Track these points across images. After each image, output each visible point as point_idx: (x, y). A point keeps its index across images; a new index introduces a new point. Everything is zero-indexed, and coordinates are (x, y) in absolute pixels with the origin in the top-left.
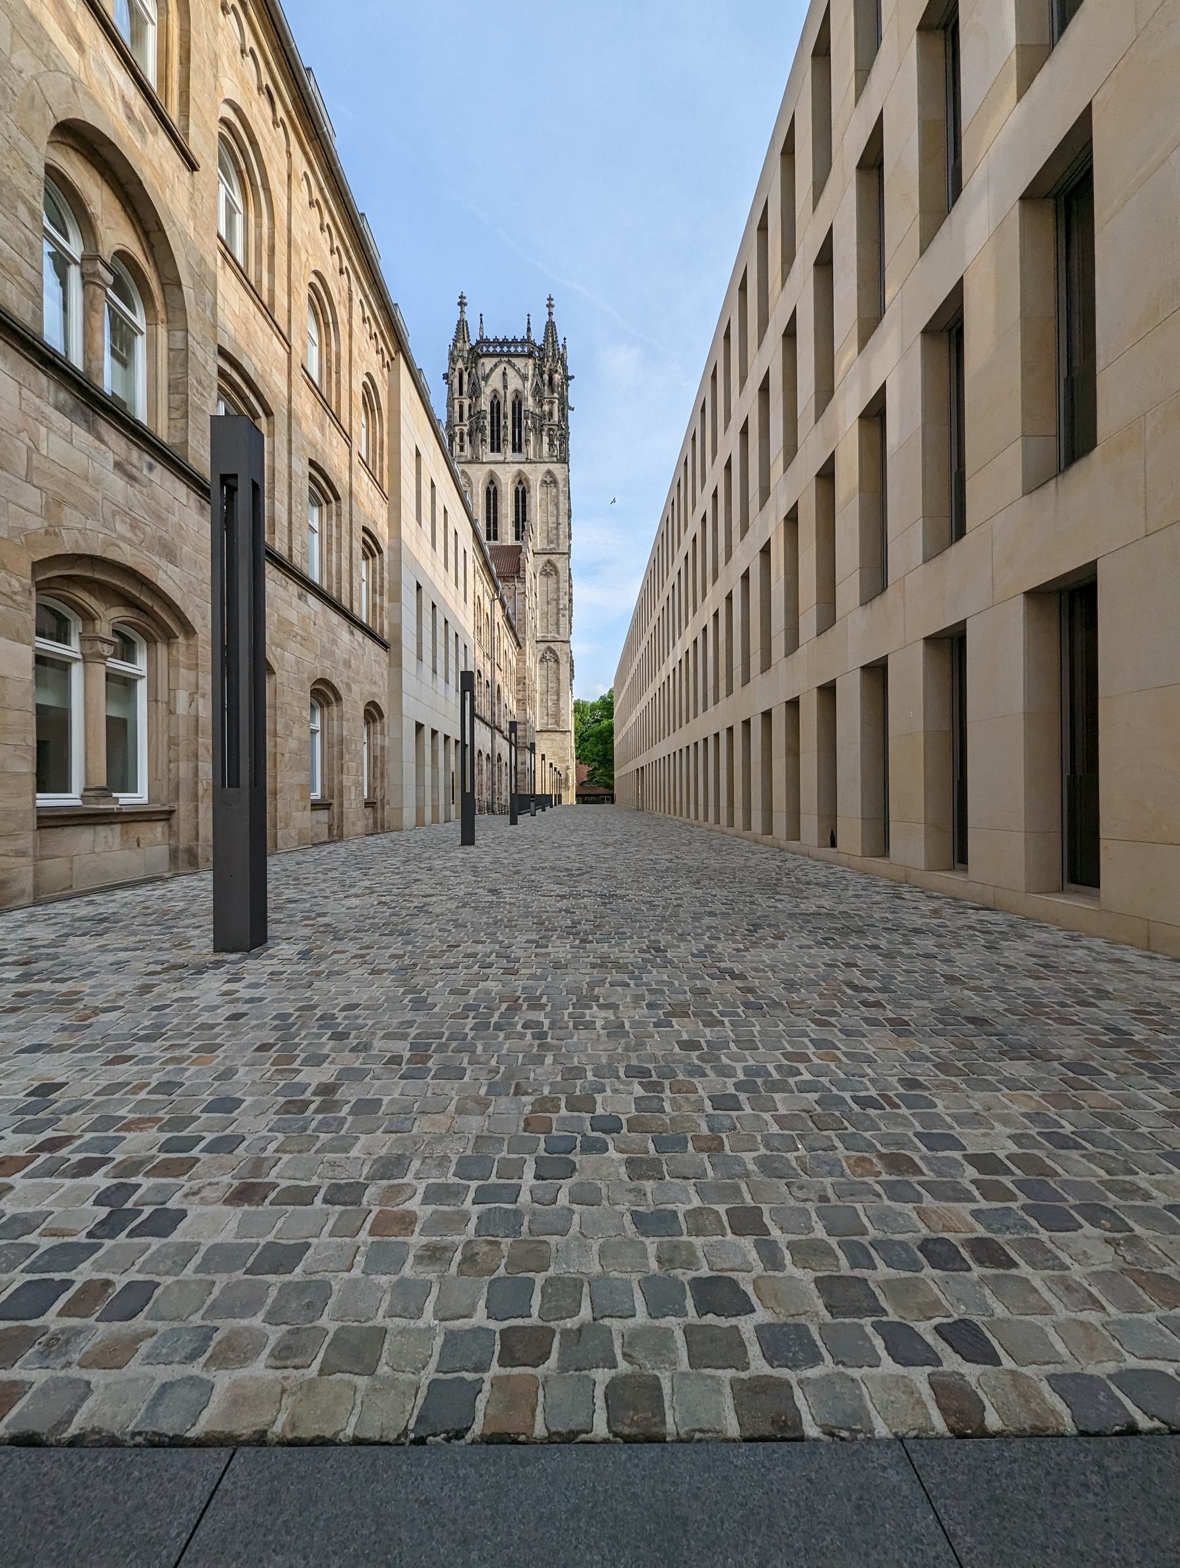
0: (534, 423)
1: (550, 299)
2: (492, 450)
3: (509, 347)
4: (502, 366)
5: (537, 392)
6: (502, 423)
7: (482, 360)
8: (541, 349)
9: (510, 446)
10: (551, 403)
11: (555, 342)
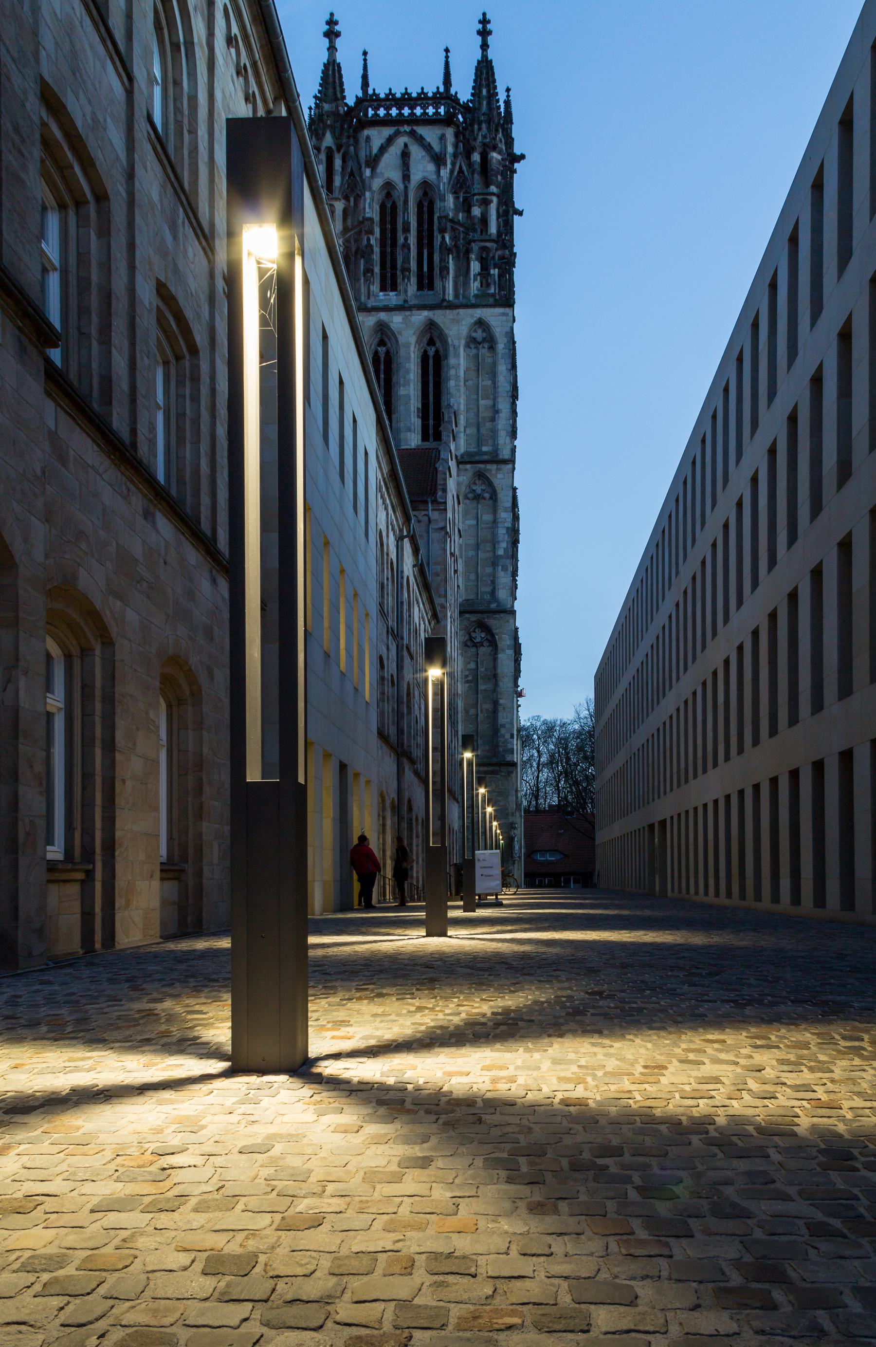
0: (454, 238)
1: (484, 21)
2: (383, 288)
3: (412, 108)
4: (401, 141)
5: (459, 184)
6: (401, 240)
7: (366, 132)
8: (465, 108)
9: (414, 280)
10: (486, 203)
11: (492, 95)
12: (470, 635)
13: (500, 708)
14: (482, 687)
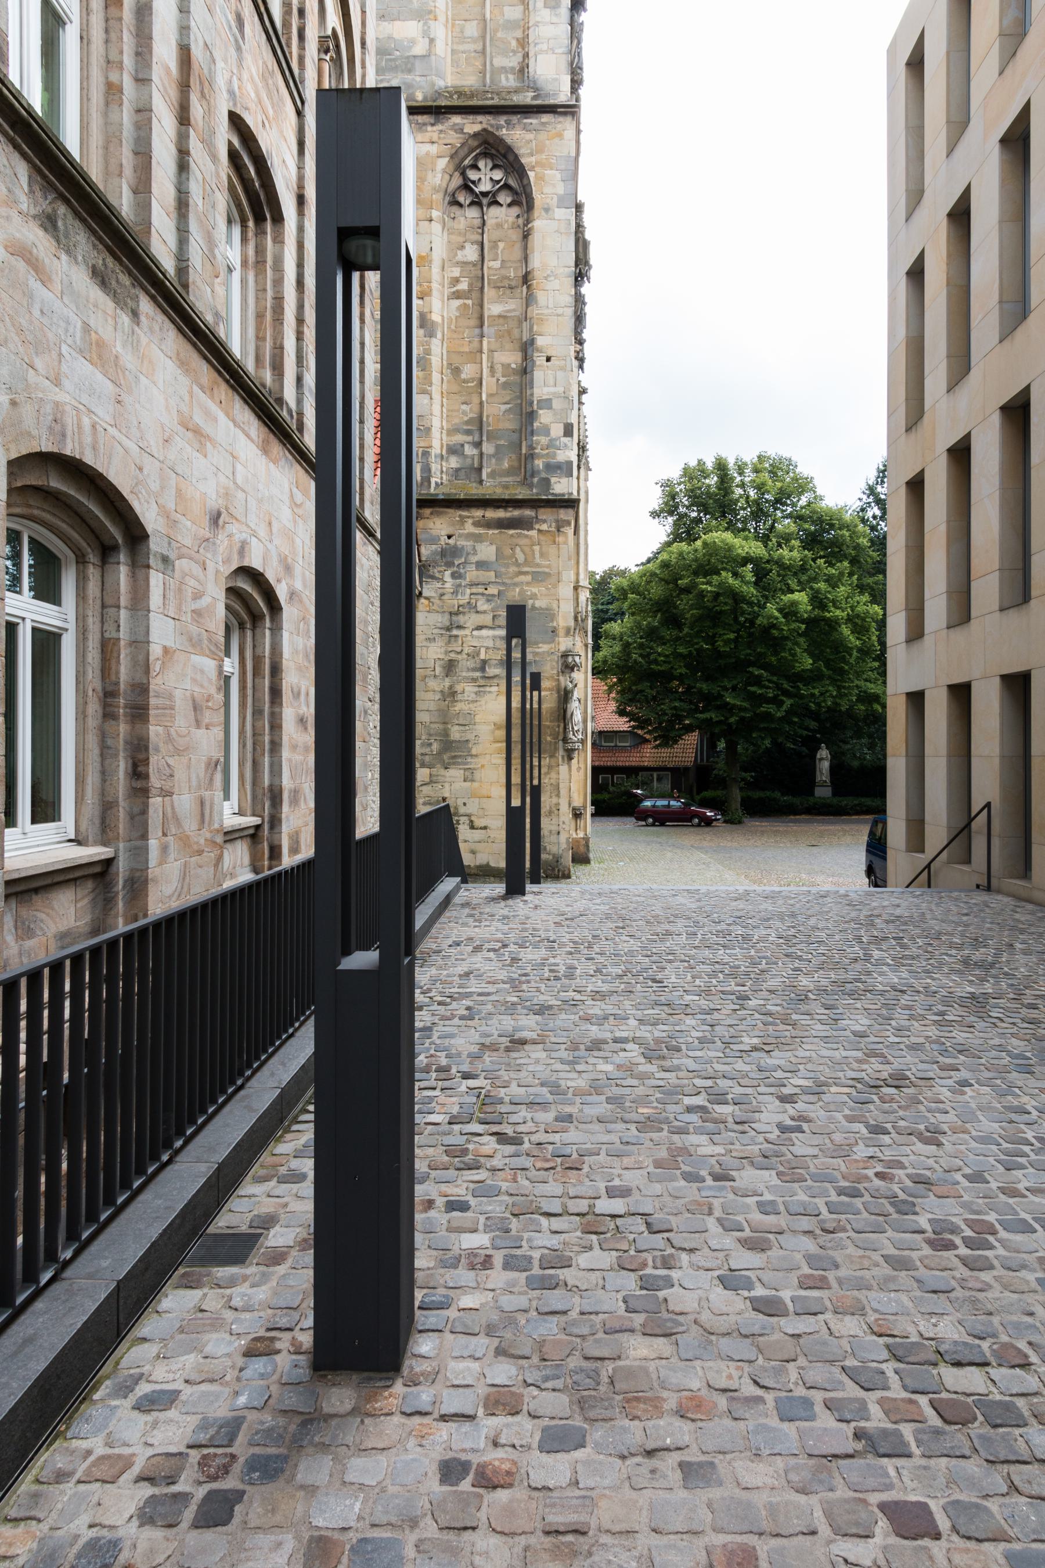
12: (463, 174)
13: (540, 360)
14: (493, 309)
